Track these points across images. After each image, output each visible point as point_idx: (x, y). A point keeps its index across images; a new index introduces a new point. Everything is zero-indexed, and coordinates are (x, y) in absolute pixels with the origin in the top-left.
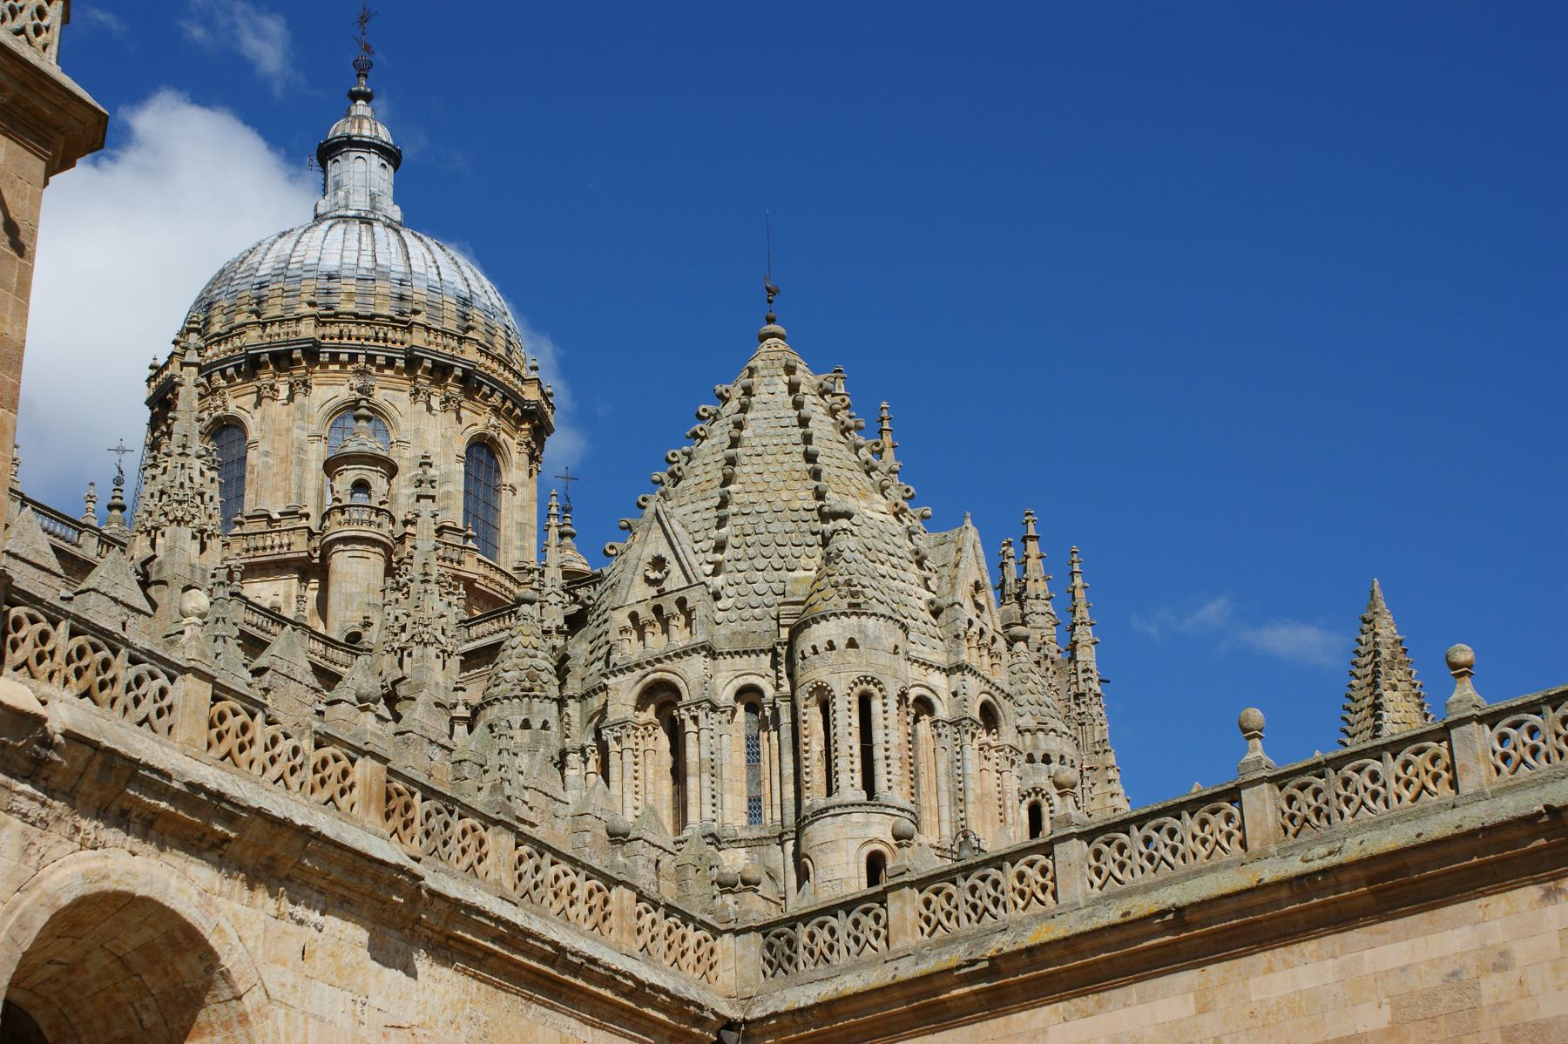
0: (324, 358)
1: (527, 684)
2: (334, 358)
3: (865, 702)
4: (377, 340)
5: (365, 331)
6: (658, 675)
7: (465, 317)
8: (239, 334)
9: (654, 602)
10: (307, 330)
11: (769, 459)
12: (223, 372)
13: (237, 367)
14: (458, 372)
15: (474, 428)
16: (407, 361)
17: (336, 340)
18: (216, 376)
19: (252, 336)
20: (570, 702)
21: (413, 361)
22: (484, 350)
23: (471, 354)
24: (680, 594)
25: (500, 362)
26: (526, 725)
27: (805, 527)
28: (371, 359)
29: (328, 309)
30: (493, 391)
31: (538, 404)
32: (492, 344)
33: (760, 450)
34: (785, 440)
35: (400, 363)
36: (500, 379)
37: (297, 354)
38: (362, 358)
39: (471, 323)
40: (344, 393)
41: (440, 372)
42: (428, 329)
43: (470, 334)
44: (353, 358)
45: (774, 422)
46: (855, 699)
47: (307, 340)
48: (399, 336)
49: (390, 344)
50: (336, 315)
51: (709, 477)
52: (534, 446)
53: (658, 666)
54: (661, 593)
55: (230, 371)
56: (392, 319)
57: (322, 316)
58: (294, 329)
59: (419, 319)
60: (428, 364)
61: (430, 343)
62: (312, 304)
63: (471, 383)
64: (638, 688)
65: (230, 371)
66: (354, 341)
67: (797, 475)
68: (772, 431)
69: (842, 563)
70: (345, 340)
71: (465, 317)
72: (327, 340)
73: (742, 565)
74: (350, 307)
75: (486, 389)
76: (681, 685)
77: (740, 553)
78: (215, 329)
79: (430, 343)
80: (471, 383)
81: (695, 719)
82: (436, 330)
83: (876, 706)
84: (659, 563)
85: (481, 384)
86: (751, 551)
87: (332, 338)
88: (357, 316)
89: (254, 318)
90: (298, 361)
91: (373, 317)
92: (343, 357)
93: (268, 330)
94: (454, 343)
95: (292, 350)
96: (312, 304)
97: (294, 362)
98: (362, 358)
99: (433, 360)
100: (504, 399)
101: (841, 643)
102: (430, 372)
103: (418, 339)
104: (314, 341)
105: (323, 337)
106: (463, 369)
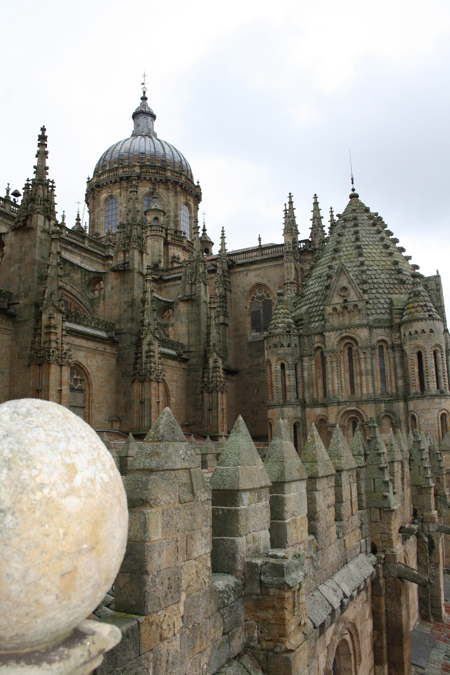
1: (288, 329)
3: (435, 353)
6: (347, 334)
9: (343, 305)
11: (371, 247)
20: (305, 337)
24: (355, 303)
26: (289, 346)
27: (393, 277)
33: (366, 243)
34: (375, 240)
45: (368, 232)
46: (432, 353)
51: (350, 252)
53: (348, 330)
54: (345, 301)
56: (161, 167)
64: (339, 338)
67: (384, 255)
68: (368, 235)
69: (421, 297)
73: (374, 291)
74: (149, 163)
76: (358, 339)
77: (372, 286)
78: (108, 168)
81: (364, 353)
83: (439, 355)
84: (345, 289)
86: (376, 286)
91: (155, 166)
101: (427, 331)
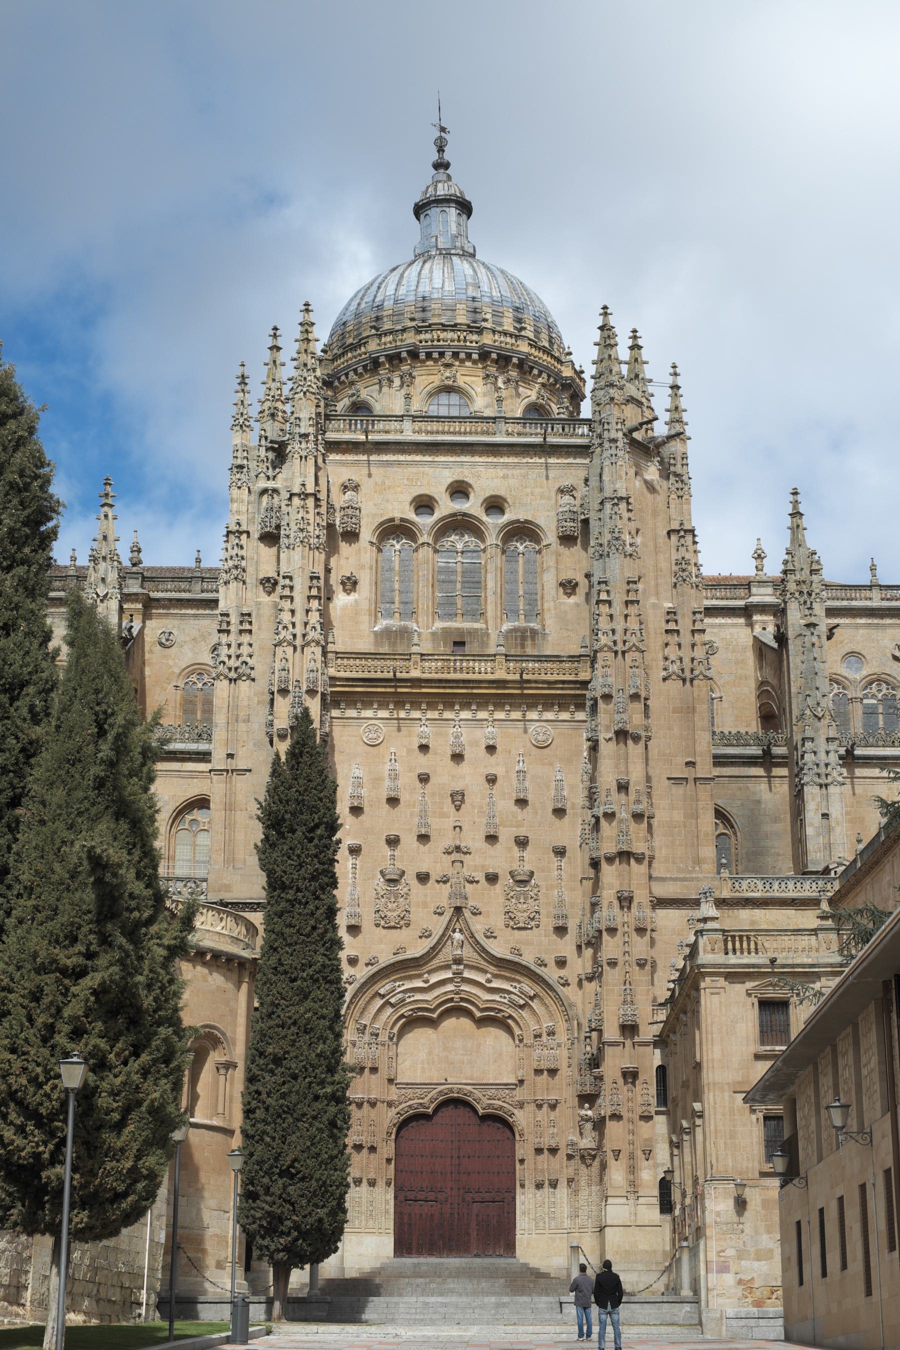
0: (422, 356)
2: (429, 356)
4: (459, 341)
5: (450, 335)
7: (519, 321)
8: (365, 343)
10: (410, 338)
12: (355, 371)
13: (365, 367)
14: (515, 360)
15: (527, 400)
16: (480, 355)
17: (430, 343)
18: (351, 374)
19: (373, 346)
21: (484, 356)
22: (533, 344)
23: (524, 347)
25: (544, 351)
28: (455, 355)
29: (423, 321)
30: (540, 372)
31: (571, 378)
32: (539, 339)
35: (475, 356)
36: (545, 363)
37: (404, 355)
38: (448, 355)
39: (523, 325)
40: (436, 380)
41: (503, 361)
42: (494, 332)
43: (523, 333)
44: (442, 355)
47: (408, 345)
48: (475, 337)
49: (468, 344)
50: (430, 326)
52: (571, 409)
55: (360, 370)
56: (469, 326)
57: (419, 327)
58: (400, 337)
59: (488, 325)
60: (494, 356)
61: (495, 341)
62: (412, 319)
63: (525, 367)
65: (360, 370)
66: (441, 343)
70: (435, 343)
71: (519, 321)
72: (424, 343)
75: (535, 372)
79: (495, 341)
80: (525, 367)
82: (499, 332)
85: (532, 368)
87: (426, 342)
88: (443, 325)
89: (373, 332)
90: (405, 358)
92: (435, 355)
93: (383, 340)
94: (513, 341)
95: (400, 353)
96: (412, 319)
97: (401, 360)
98: (448, 355)
99: (498, 354)
100: (549, 376)
102: (496, 362)
103: (487, 339)
104: (414, 345)
105: (421, 342)
106: (519, 358)
